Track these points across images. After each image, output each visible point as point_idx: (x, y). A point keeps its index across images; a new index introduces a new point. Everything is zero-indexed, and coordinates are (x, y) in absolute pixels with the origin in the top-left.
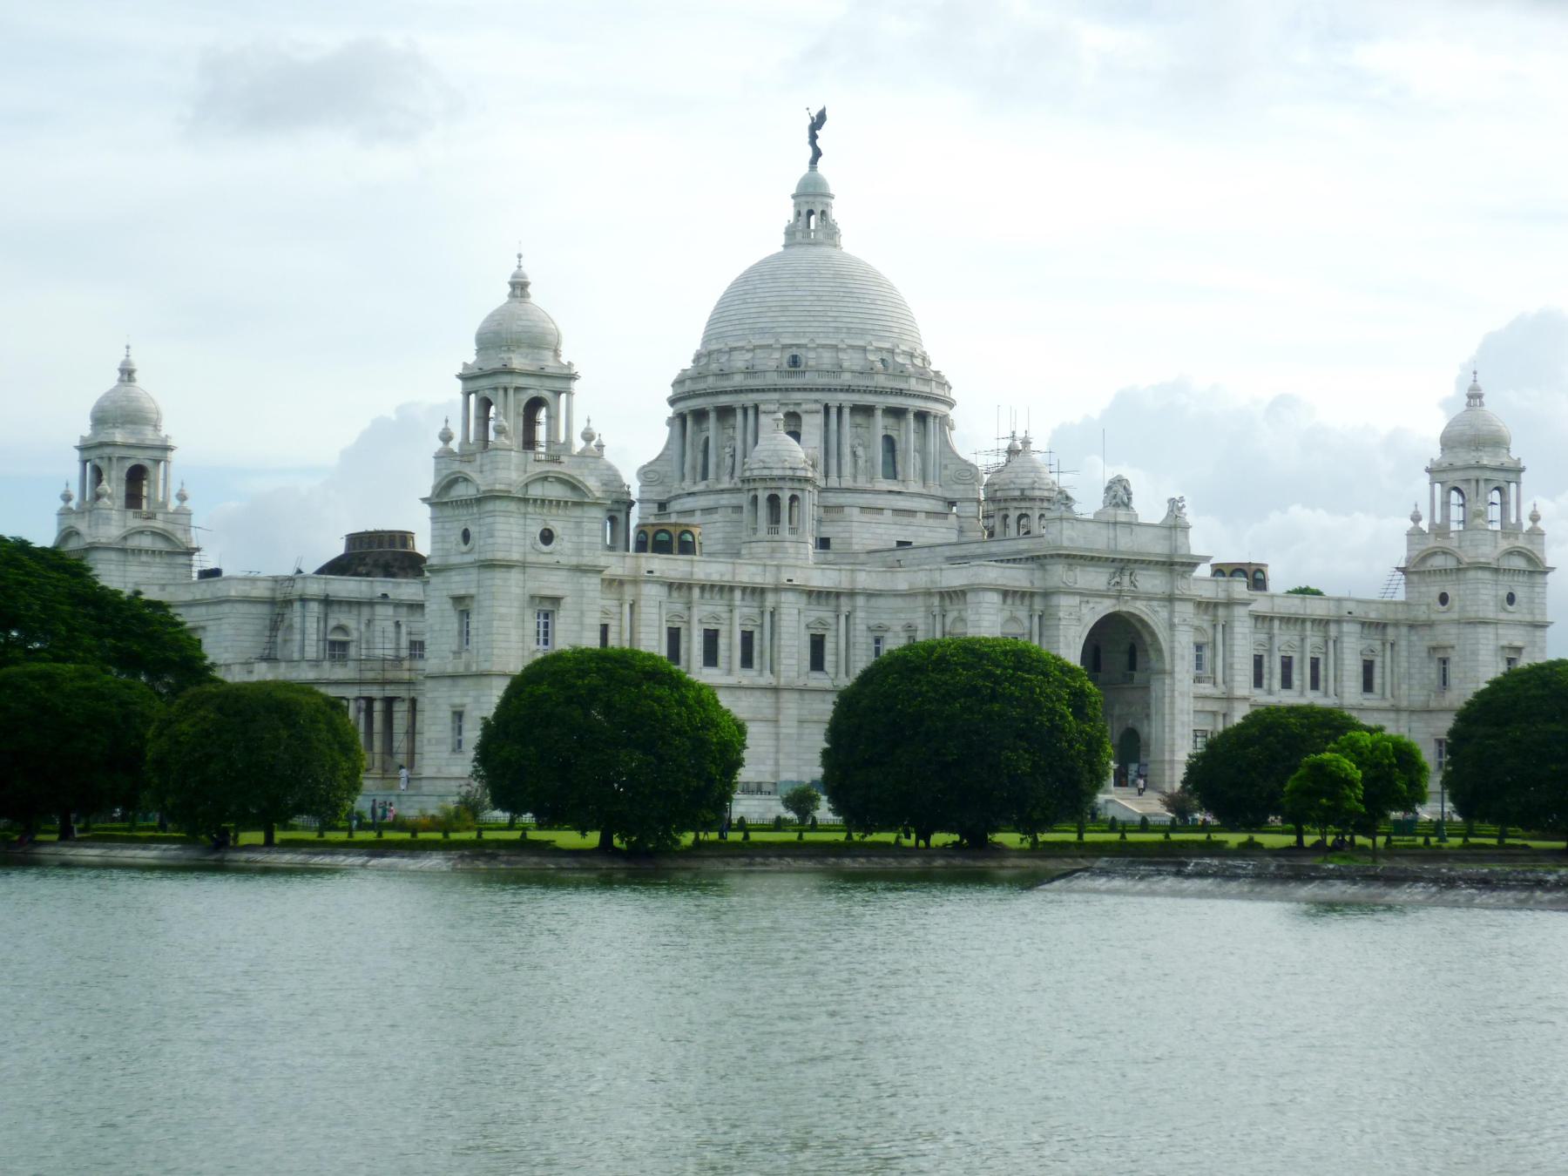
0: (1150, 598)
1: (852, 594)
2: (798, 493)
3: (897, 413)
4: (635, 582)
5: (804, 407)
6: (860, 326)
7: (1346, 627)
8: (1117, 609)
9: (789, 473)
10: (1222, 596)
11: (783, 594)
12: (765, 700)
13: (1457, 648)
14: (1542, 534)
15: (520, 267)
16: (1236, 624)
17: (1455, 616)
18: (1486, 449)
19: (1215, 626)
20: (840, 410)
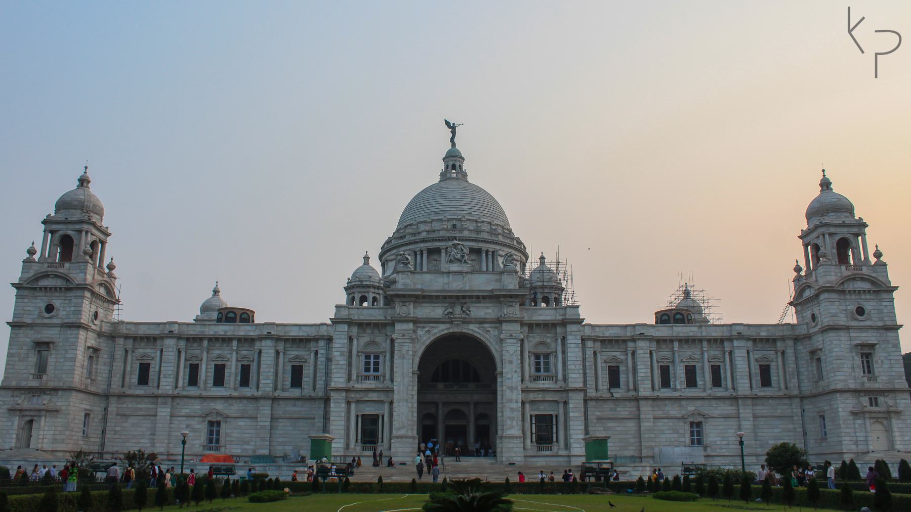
0: (481, 322)
1: (316, 339)
2: (366, 294)
4: (162, 338)
6: (443, 209)
7: (736, 343)
8: (451, 330)
9: (359, 283)
10: (559, 318)
11: (263, 341)
12: (250, 405)
13: (823, 350)
14: (885, 265)
15: (85, 173)
16: (569, 337)
17: (816, 329)
18: (830, 214)
19: (557, 340)
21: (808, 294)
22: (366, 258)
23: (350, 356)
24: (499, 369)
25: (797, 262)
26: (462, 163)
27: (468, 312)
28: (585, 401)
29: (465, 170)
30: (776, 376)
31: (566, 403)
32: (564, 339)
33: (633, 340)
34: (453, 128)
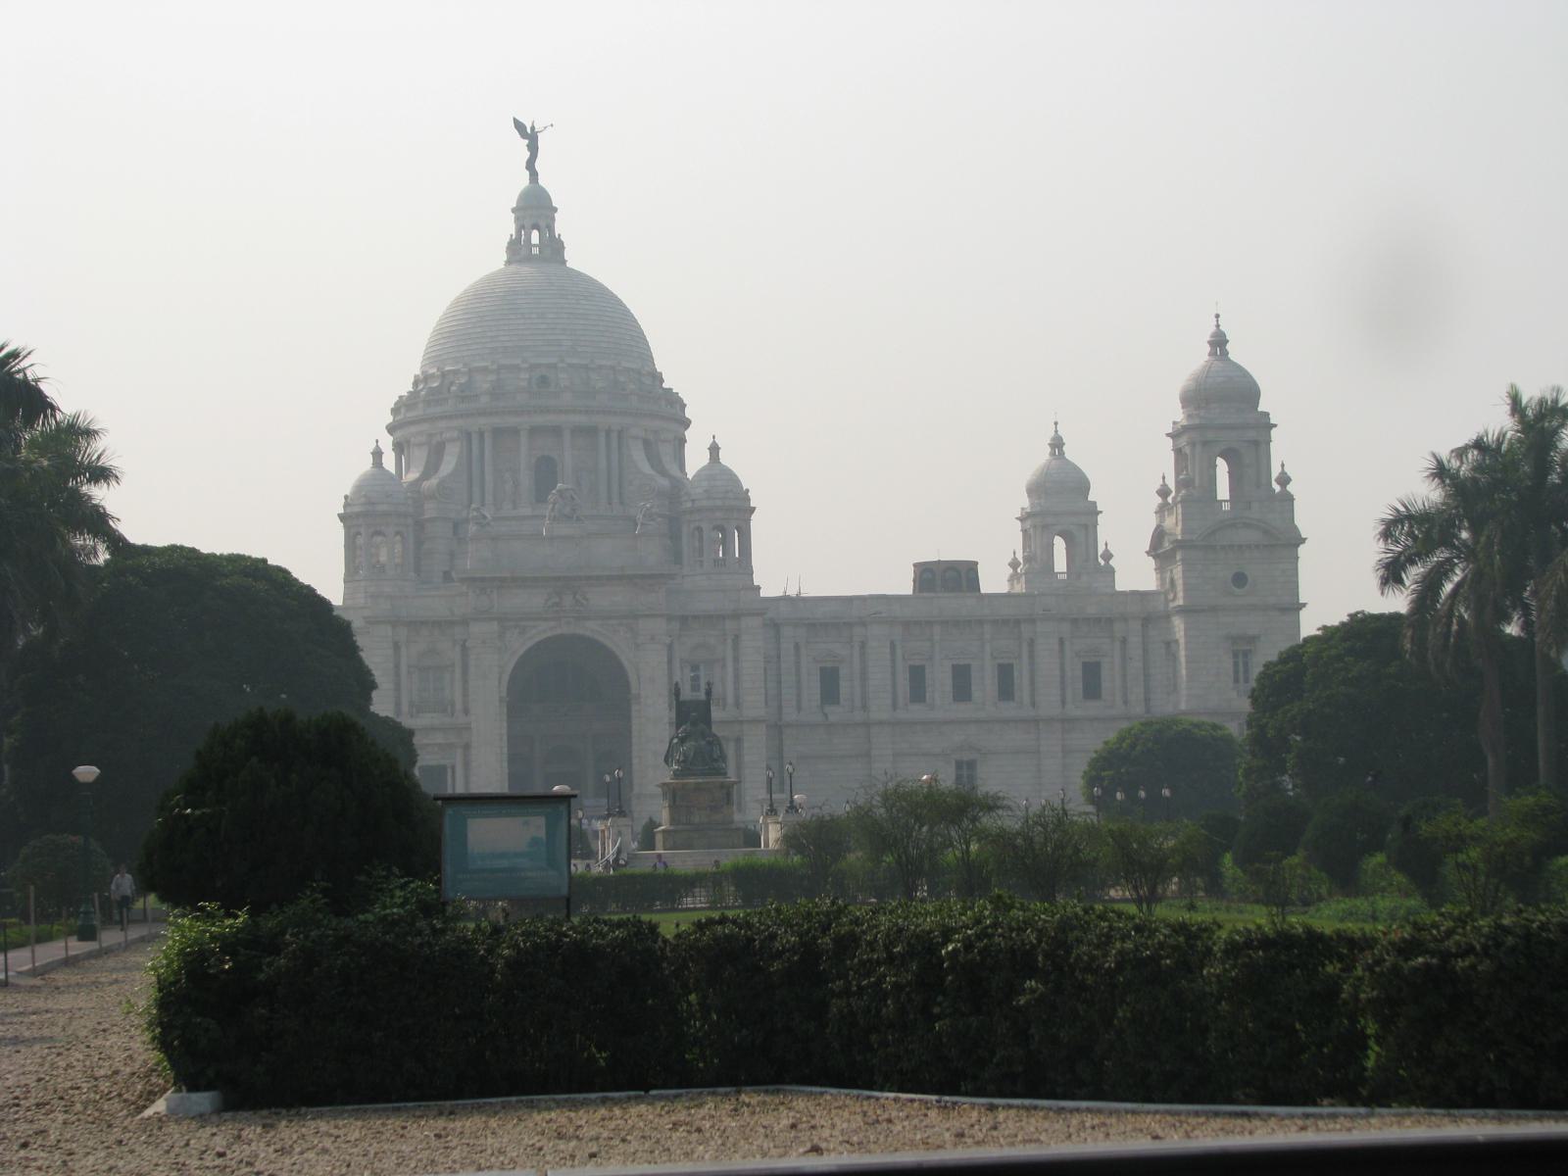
3: (556, 431)
5: (444, 436)
8: (559, 631)
14: (1290, 499)
20: (481, 435)
21: (1167, 545)
22: (377, 454)
23: (397, 674)
24: (634, 691)
25: (1164, 478)
26: (553, 219)
27: (584, 602)
28: (777, 728)
29: (559, 235)
30: (1109, 680)
31: (739, 741)
32: (737, 638)
33: (863, 624)
34: (531, 138)
